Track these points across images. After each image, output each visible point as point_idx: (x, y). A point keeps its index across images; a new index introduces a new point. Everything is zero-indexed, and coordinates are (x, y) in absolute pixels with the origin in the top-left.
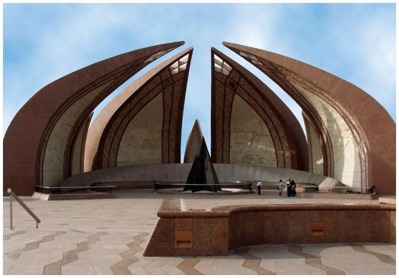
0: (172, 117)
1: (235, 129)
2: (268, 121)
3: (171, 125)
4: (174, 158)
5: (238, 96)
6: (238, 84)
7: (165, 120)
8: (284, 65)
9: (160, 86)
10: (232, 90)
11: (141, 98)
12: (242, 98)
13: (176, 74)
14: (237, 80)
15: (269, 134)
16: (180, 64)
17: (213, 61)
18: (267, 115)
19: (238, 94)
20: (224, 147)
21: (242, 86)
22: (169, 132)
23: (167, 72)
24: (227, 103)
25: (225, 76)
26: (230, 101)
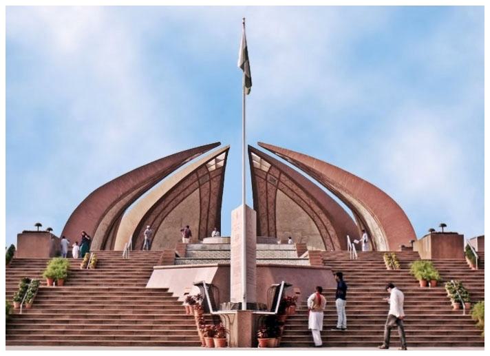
0: (210, 215)
2: (316, 218)
3: (209, 224)
5: (281, 193)
6: (279, 179)
9: (197, 183)
12: (285, 193)
14: (278, 176)
15: (318, 232)
16: (217, 161)
17: (251, 158)
18: (316, 213)
23: (203, 169)
24: (270, 200)
26: (273, 197)
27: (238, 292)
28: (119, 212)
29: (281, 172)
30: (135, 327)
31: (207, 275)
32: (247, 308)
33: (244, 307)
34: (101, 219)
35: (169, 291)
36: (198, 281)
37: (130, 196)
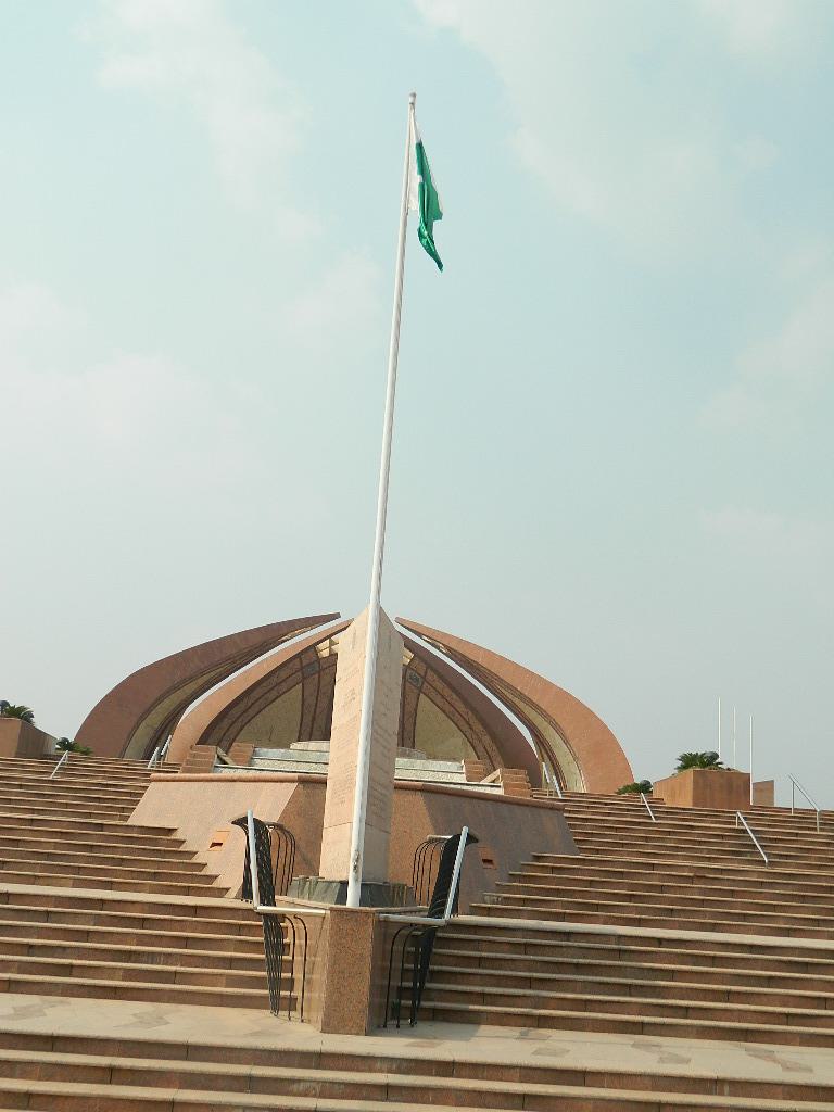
2: (476, 742)
6: (424, 677)
8: (480, 661)
9: (299, 674)
24: (409, 708)
27: (341, 850)
28: (174, 710)
29: (429, 666)
30: (40, 933)
31: (270, 804)
32: (363, 902)
33: (352, 901)
34: (142, 718)
35: (177, 836)
36: (238, 815)
37: (192, 687)
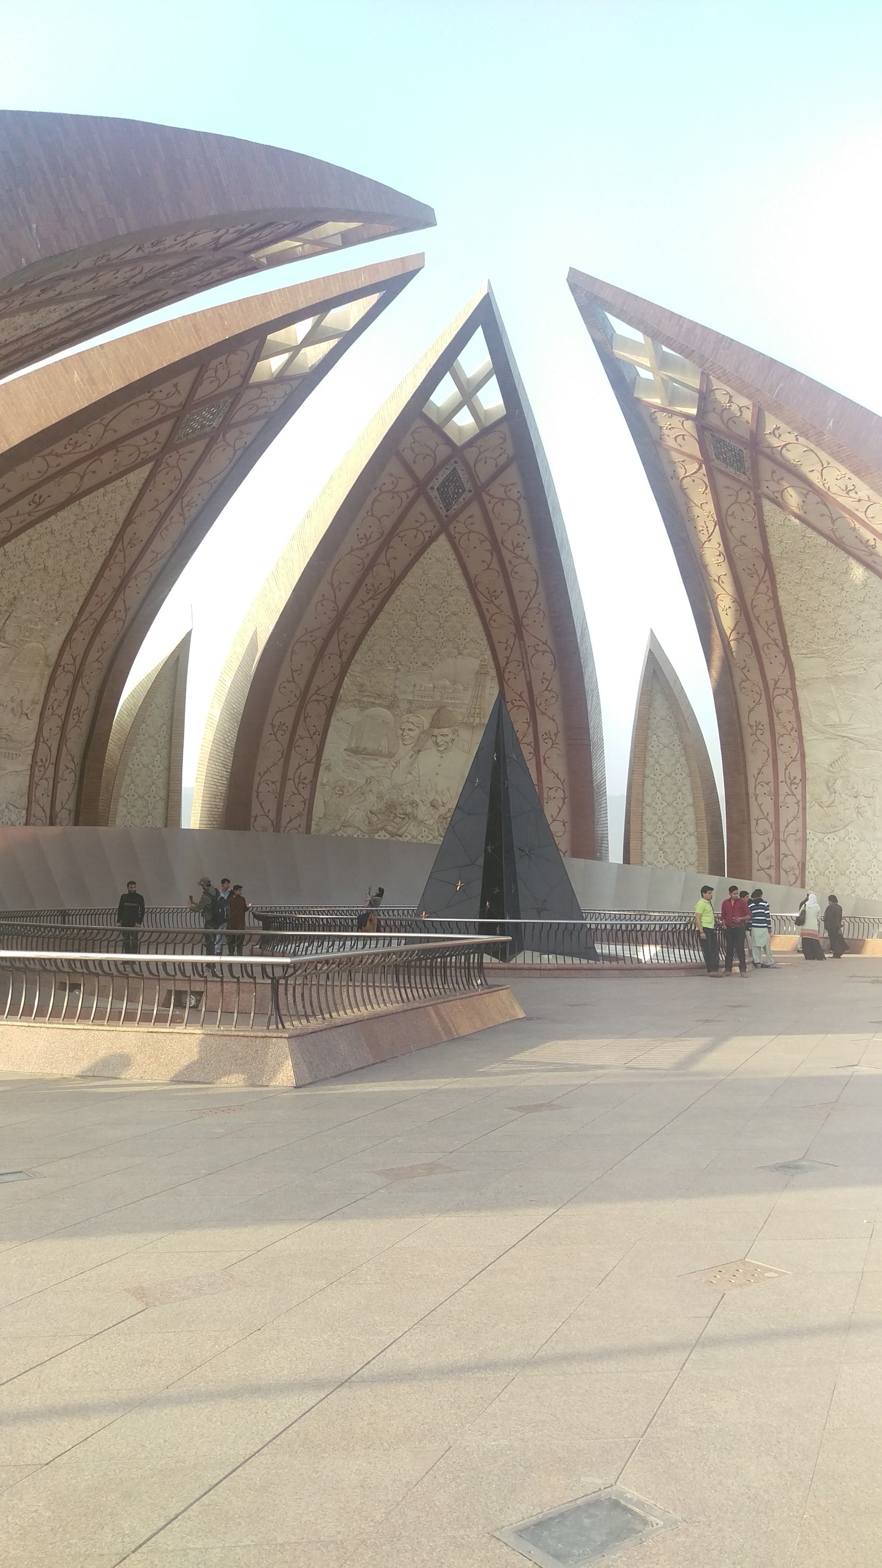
0: (119, 605)
1: (362, 688)
3: (97, 644)
4: (71, 805)
5: (447, 546)
6: (480, 491)
7: (85, 615)
10: (436, 513)
11: (51, 471)
13: (260, 385)
19: (451, 539)
20: (293, 764)
21: (489, 507)
22: (78, 676)
25: (448, 441)
